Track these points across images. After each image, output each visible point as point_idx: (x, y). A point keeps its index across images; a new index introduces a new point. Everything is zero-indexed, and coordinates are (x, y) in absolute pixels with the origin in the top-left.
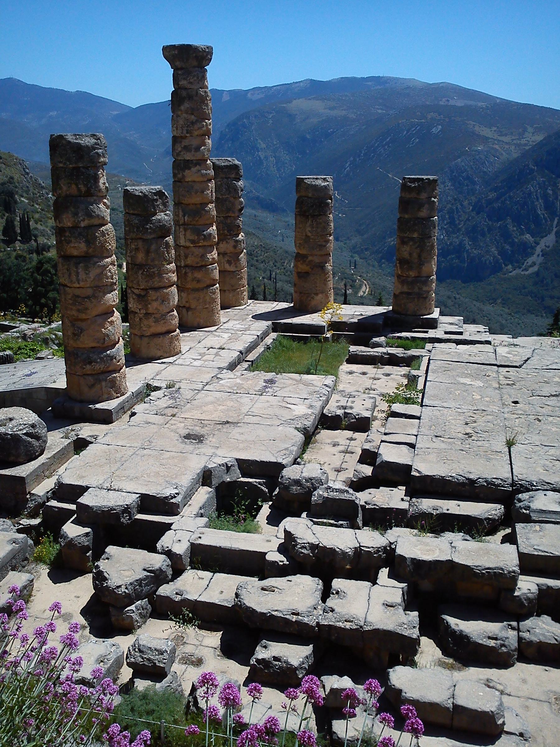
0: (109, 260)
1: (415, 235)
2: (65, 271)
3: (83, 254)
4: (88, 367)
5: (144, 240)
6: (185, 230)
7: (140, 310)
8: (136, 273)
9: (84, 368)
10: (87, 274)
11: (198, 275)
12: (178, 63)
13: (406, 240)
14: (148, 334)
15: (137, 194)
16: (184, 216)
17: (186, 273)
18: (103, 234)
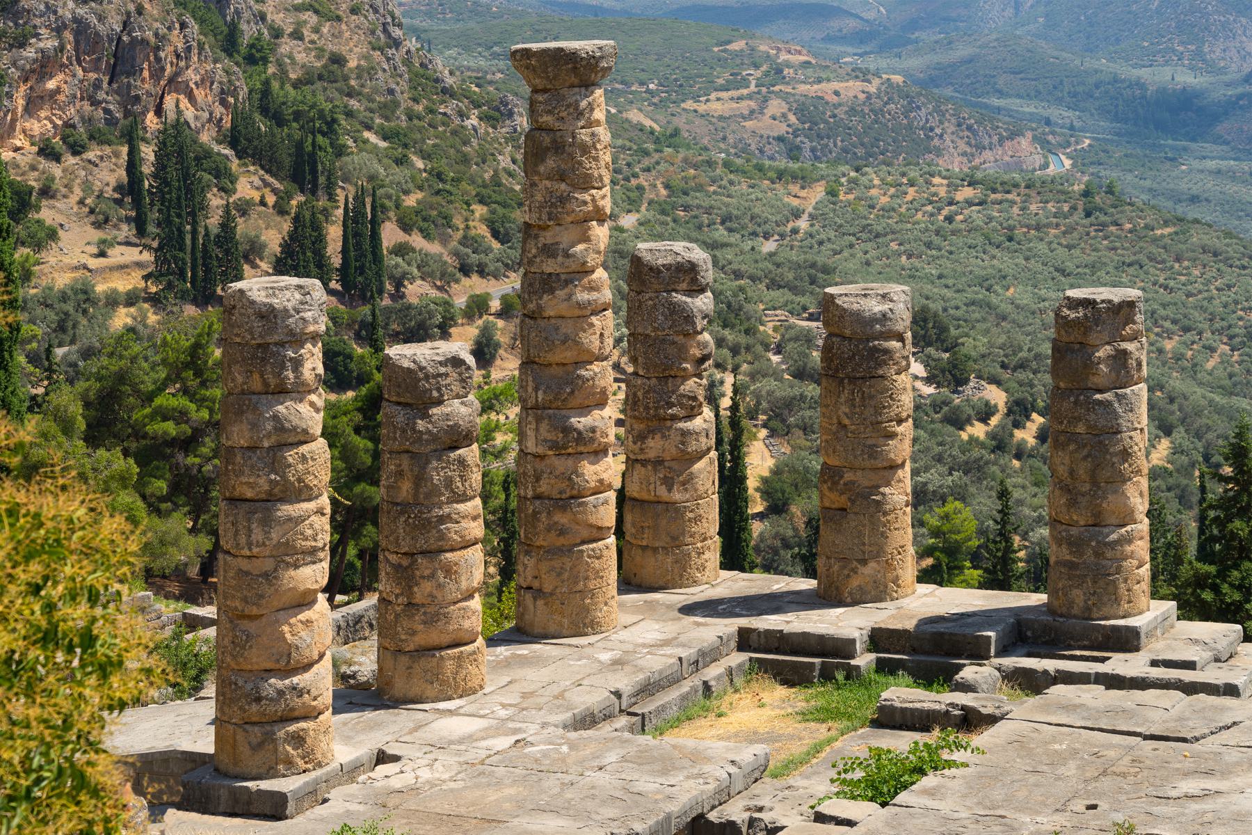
0: (311, 506)
1: (1081, 429)
2: (229, 525)
3: (263, 496)
5: (413, 455)
10: (266, 533)
11: (562, 519)
14: (412, 647)
18: (304, 458)
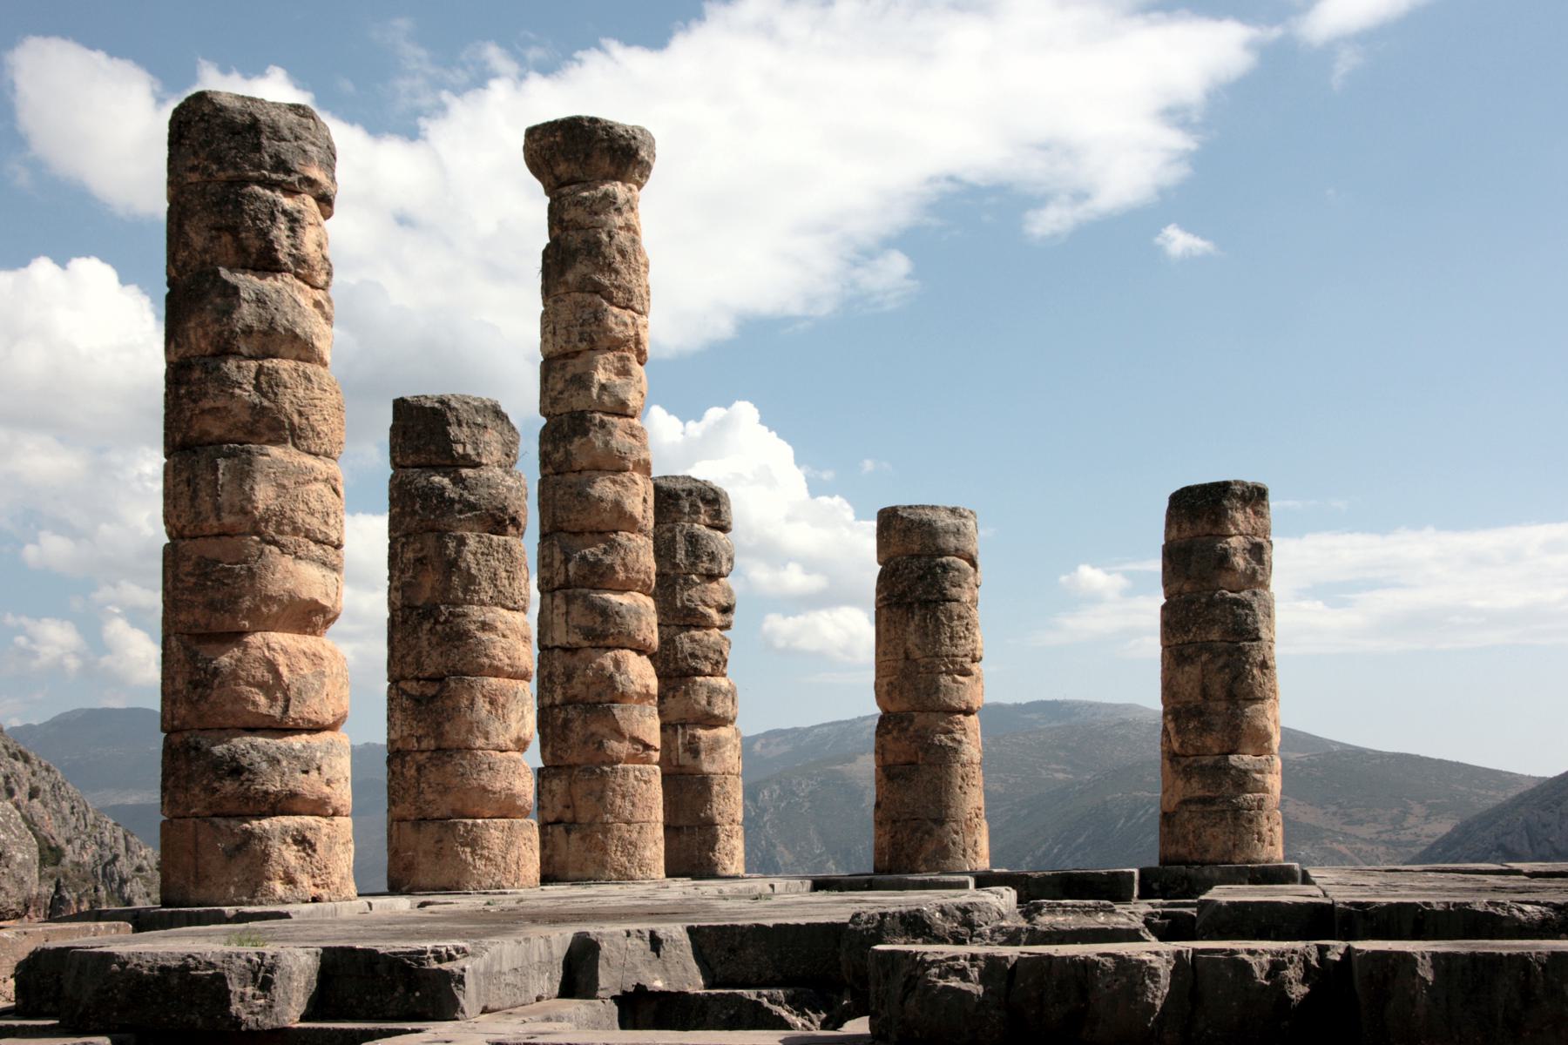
1: (1215, 635)
4: (229, 786)
6: (569, 600)
7: (419, 740)
8: (415, 630)
9: (215, 790)
12: (562, 169)
13: (1189, 651)
15: (428, 404)
16: (567, 561)
17: (566, 723)
